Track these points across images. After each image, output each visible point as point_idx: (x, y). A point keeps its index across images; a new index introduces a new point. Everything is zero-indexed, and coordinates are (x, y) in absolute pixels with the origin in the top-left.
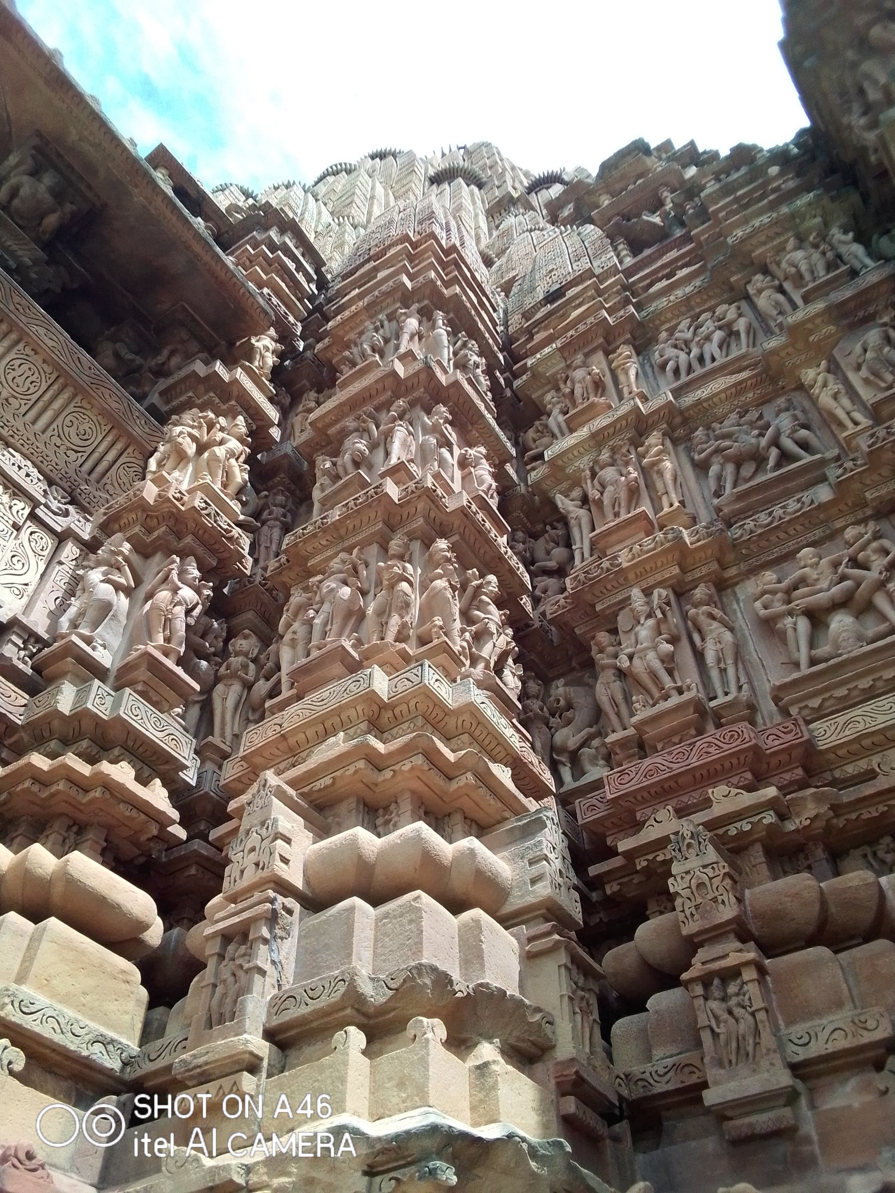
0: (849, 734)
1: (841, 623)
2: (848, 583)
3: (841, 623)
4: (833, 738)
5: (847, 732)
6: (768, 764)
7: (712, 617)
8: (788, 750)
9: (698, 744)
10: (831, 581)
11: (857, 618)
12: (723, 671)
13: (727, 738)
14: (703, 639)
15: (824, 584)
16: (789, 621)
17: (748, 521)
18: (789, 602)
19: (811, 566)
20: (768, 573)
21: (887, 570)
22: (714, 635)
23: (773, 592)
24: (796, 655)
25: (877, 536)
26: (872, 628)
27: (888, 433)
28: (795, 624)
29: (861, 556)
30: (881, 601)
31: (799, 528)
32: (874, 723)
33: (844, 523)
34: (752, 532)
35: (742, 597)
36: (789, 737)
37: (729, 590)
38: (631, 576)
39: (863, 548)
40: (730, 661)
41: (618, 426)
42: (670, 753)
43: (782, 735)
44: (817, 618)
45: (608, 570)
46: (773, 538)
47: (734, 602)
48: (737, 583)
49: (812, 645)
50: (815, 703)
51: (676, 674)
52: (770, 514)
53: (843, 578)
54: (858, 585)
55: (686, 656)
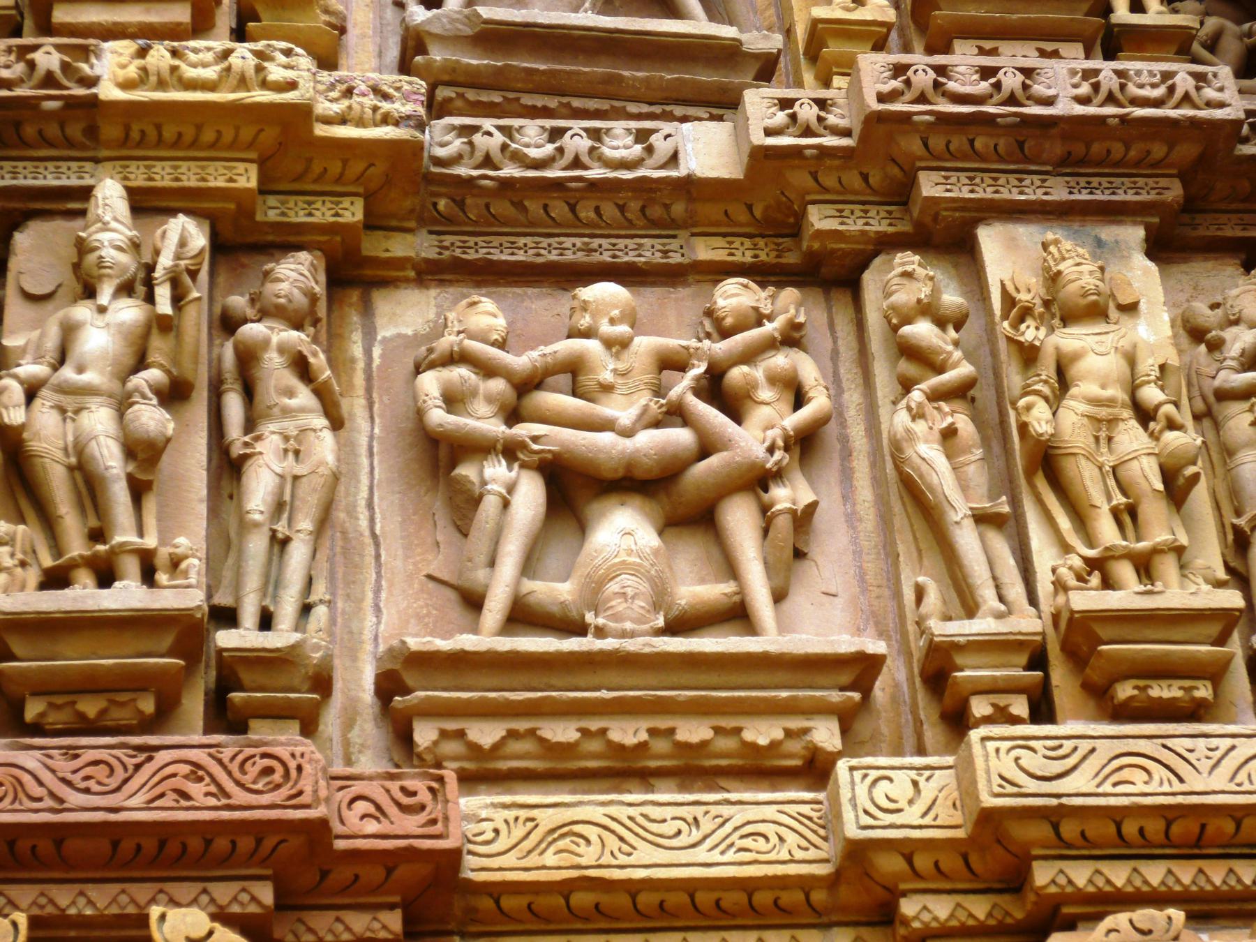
0: (552, 864)
2: (681, 437)
4: (510, 860)
5: (550, 859)
6: (324, 874)
7: (302, 367)
8: (389, 860)
9: (162, 757)
10: (646, 409)
13: (253, 771)
14: (250, 425)
16: (497, 471)
17: (488, 124)
18: (513, 416)
19: (609, 343)
20: (487, 304)
21: (787, 449)
22: (291, 427)
23: (487, 370)
24: (481, 574)
25: (792, 338)
26: (697, 589)
27: (937, 85)
28: (511, 488)
29: (737, 374)
30: (740, 519)
31: (609, 211)
32: (623, 859)
33: (720, 255)
34: (488, 162)
35: (385, 331)
36: (411, 823)
37: (355, 295)
38: (111, 131)
39: (749, 356)
40: (306, 524)
42: (72, 753)
43: (392, 810)
44: (573, 490)
45: (49, 80)
46: (534, 207)
49: (529, 566)
50: (486, 734)
52: (556, 134)
53: (676, 414)
54: (704, 451)
55: (191, 463)
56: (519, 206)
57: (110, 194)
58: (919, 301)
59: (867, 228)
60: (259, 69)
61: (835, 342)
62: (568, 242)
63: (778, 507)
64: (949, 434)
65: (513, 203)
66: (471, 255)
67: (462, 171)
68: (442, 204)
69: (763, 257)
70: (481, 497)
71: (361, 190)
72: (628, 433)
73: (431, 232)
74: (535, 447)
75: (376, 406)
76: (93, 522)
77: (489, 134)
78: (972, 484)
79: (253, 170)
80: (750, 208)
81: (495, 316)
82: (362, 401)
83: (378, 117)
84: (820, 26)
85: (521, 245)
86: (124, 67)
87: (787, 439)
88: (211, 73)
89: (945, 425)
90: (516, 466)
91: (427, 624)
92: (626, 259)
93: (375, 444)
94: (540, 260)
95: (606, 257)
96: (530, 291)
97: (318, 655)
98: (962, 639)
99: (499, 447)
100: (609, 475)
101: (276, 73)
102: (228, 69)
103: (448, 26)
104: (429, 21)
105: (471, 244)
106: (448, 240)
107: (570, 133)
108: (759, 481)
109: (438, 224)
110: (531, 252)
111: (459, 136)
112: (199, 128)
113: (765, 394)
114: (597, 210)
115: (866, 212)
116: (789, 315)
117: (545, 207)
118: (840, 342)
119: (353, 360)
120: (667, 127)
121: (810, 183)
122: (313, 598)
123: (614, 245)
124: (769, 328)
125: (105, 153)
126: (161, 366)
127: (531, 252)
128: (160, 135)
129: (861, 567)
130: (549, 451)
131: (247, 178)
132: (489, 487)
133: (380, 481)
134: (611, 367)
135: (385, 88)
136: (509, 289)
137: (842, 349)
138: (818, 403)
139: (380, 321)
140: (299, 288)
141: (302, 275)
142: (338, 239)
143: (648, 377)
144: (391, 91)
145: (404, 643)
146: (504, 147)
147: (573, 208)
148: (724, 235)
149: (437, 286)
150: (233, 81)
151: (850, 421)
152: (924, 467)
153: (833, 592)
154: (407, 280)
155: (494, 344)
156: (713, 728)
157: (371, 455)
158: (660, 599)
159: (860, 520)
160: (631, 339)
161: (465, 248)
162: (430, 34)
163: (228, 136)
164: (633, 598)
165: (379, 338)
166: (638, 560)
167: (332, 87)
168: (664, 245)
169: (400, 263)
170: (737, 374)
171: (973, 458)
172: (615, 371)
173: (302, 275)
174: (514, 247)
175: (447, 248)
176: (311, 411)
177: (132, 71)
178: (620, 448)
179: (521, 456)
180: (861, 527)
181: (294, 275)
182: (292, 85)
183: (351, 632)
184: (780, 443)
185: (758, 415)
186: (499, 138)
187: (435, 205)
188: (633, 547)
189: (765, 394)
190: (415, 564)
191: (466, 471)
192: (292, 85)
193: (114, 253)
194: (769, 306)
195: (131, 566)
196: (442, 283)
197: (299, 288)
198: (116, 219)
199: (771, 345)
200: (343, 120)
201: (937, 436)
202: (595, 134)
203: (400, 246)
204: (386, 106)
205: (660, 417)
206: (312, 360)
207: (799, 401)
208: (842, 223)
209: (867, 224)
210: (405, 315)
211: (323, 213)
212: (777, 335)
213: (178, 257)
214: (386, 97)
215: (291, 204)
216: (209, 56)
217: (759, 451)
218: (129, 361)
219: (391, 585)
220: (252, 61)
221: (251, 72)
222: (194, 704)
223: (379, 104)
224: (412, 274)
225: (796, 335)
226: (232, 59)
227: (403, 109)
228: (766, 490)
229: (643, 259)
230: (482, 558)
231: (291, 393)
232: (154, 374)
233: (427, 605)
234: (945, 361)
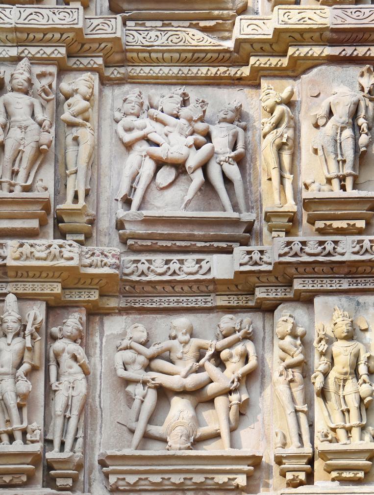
7: (75, 358)
10: (192, 367)
12: (67, 419)
15: (181, 368)
18: (148, 368)
22: (71, 379)
23: (139, 353)
29: (224, 354)
38: (11, 273)
39: (230, 346)
40: (75, 412)
41: (49, 36)
46: (159, 288)
48: (107, 314)
49: (150, 421)
51: (25, 411)
52: (167, 262)
53: (201, 369)
56: (154, 288)
57: (11, 299)
59: (277, 296)
60: (60, 252)
61: (264, 334)
62: (172, 299)
65: (152, 287)
66: (137, 305)
67: (134, 278)
68: (127, 288)
69: (241, 304)
70: (134, 399)
71: (98, 287)
72: (186, 377)
73: (124, 296)
75: (103, 361)
76: (7, 418)
77: (143, 263)
79: (60, 285)
80: (237, 286)
81: (143, 332)
83: (103, 264)
84: (268, 214)
85: (155, 301)
86: (15, 252)
88: (43, 255)
92: (192, 305)
94: (161, 306)
95: (185, 305)
97: (78, 459)
99: (141, 382)
101: (66, 254)
102: (50, 252)
103: (132, 218)
104: (125, 216)
105: (137, 301)
106: (130, 299)
107: (173, 262)
109: (126, 294)
110: (158, 303)
111: (133, 263)
112: (41, 273)
114: (182, 288)
115: (276, 290)
116: (245, 330)
117: (163, 288)
120: (207, 257)
121: (257, 280)
122: (78, 436)
123: (188, 300)
124: (238, 335)
125: (10, 280)
126: (28, 363)
127: (158, 303)
128: (28, 274)
131: (57, 289)
133: (103, 388)
134: (181, 351)
135: (105, 253)
136: (151, 315)
137: (266, 337)
138: (253, 361)
140: (75, 329)
142: (90, 304)
144: (107, 254)
145: (106, 452)
146: (149, 268)
147: (173, 288)
148: (227, 295)
149: (126, 315)
150: (51, 257)
154: (115, 313)
155: (141, 344)
156: (205, 478)
161: (135, 303)
162: (125, 220)
163: (51, 274)
164: (181, 436)
167: (87, 253)
168: (205, 299)
169: (113, 309)
174: (152, 301)
175: (129, 302)
176: (78, 373)
177: (17, 255)
181: (73, 324)
182: (72, 259)
184: (236, 380)
186: (147, 265)
187: (125, 288)
189: (236, 359)
191: (130, 388)
192: (72, 259)
193: (12, 324)
195: (18, 435)
196: (127, 314)
197: (75, 329)
198: (13, 311)
199: (238, 341)
200: (91, 266)
202: (181, 262)
203: (113, 303)
204: (105, 260)
205: (197, 369)
206: (78, 356)
207: (246, 361)
208: (268, 295)
209: (277, 295)
210: (114, 326)
211: (84, 297)
212: (240, 337)
213: (33, 324)
214: (106, 256)
215: (74, 293)
216: (43, 248)
218: (18, 361)
220: (58, 249)
221: (57, 254)
222: (40, 475)
223: (103, 259)
224: (117, 311)
225: (249, 336)
226: (52, 249)
227: (111, 262)
229: (197, 306)
230: (134, 419)
231: (71, 367)
232: (26, 367)
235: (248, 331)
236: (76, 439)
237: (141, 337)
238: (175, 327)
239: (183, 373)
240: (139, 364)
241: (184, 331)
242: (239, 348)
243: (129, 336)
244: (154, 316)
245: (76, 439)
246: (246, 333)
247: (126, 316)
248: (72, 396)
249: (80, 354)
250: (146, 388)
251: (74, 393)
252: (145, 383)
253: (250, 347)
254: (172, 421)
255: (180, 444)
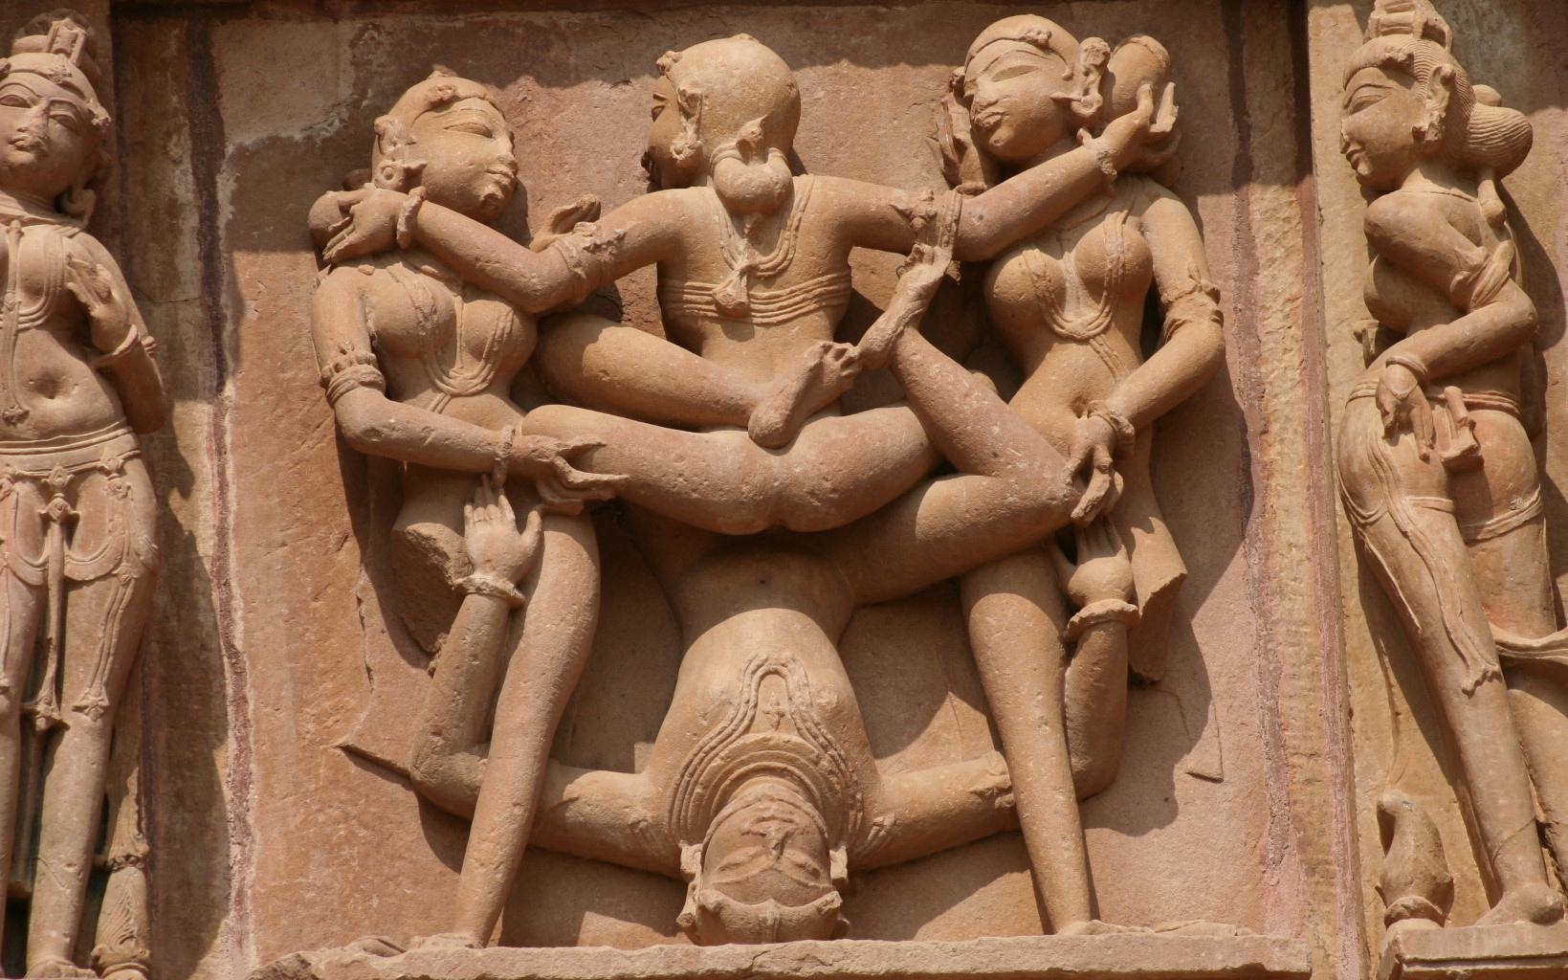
1: (758, 664)
2: (888, 431)
3: (758, 664)
10: (817, 370)
11: (843, 641)
19: (738, 208)
22: (55, 465)
23: (472, 279)
25: (1148, 169)
28: (526, 575)
29: (1020, 272)
30: (1008, 623)
35: (241, 137)
37: (172, 40)
39: (1051, 224)
44: (659, 560)
47: (180, 147)
53: (878, 382)
58: (1418, 134)
61: (1244, 140)
63: (1094, 608)
64: (1463, 478)
70: (461, 594)
72: (778, 441)
74: (578, 476)
78: (1509, 580)
81: (488, 134)
82: (196, 312)
87: (1119, 447)
89: (1453, 452)
90: (534, 518)
91: (346, 862)
93: (227, 422)
96: (563, 19)
98: (1460, 969)
99: (500, 476)
100: (731, 525)
108: (1051, 543)
113: (1081, 315)
118: (1256, 139)
119: (174, 208)
122: (116, 851)
124: (1093, 150)
129: (1274, 711)
130: (608, 484)
132: (478, 577)
134: (742, 262)
136: (518, 16)
139: (230, 107)
140: (63, 120)
141: (67, 86)
143: (817, 284)
145: (305, 963)
151: (1268, 343)
152: (1405, 550)
153: (1213, 772)
157: (220, 451)
158: (838, 808)
159: (1281, 592)
160: (788, 190)
164: (781, 846)
165: (230, 149)
166: (795, 738)
170: (1020, 272)
171: (1515, 521)
172: (750, 273)
173: (67, 86)
176: (99, 424)
178: (757, 479)
179: (547, 495)
180: (1280, 608)
181: (49, 88)
183: (186, 884)
184: (1104, 457)
185: (1058, 369)
188: (785, 707)
189: (1081, 315)
190: (318, 718)
194: (1095, 95)
197: (63, 120)
199: (1091, 195)
201: (1439, 473)
206: (98, 310)
212: (1107, 168)
217: (1053, 479)
219: (269, 773)
225: (1154, 158)
228: (1074, 559)
231: (49, 385)
233: (347, 817)
234: (1467, 286)
235: (1155, 128)
236: (96, 878)
237: (481, 170)
238: (689, 106)
239: (769, 414)
240: (477, 352)
241: (752, 128)
242: (1109, 237)
243: (391, 160)
244: (539, 19)
245: (96, 878)
246: (1142, 138)
247: (359, 24)
248: (68, 584)
249: (107, 299)
250: (534, 518)
251: (81, 563)
252: (525, 483)
253: (1165, 232)
254: (709, 738)
255: (780, 898)
